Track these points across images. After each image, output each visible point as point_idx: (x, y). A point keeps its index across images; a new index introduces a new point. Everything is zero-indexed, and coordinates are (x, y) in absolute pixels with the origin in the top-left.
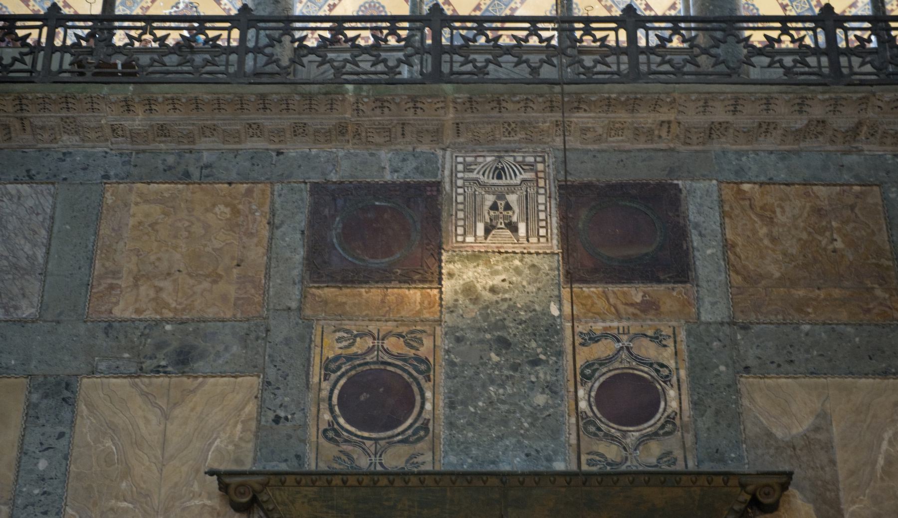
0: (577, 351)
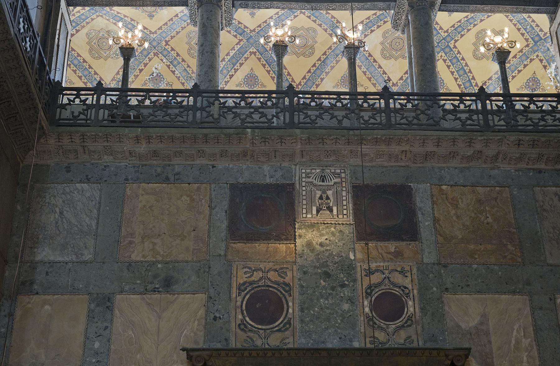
0: (363, 279)
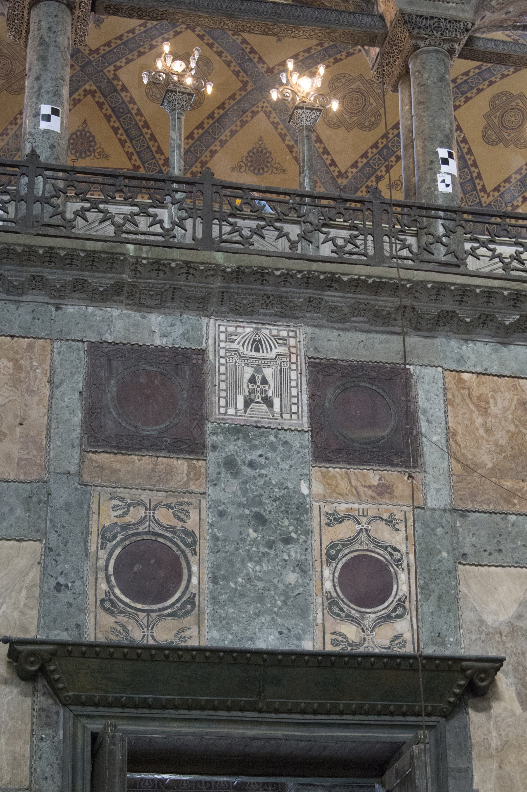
0: (323, 531)
